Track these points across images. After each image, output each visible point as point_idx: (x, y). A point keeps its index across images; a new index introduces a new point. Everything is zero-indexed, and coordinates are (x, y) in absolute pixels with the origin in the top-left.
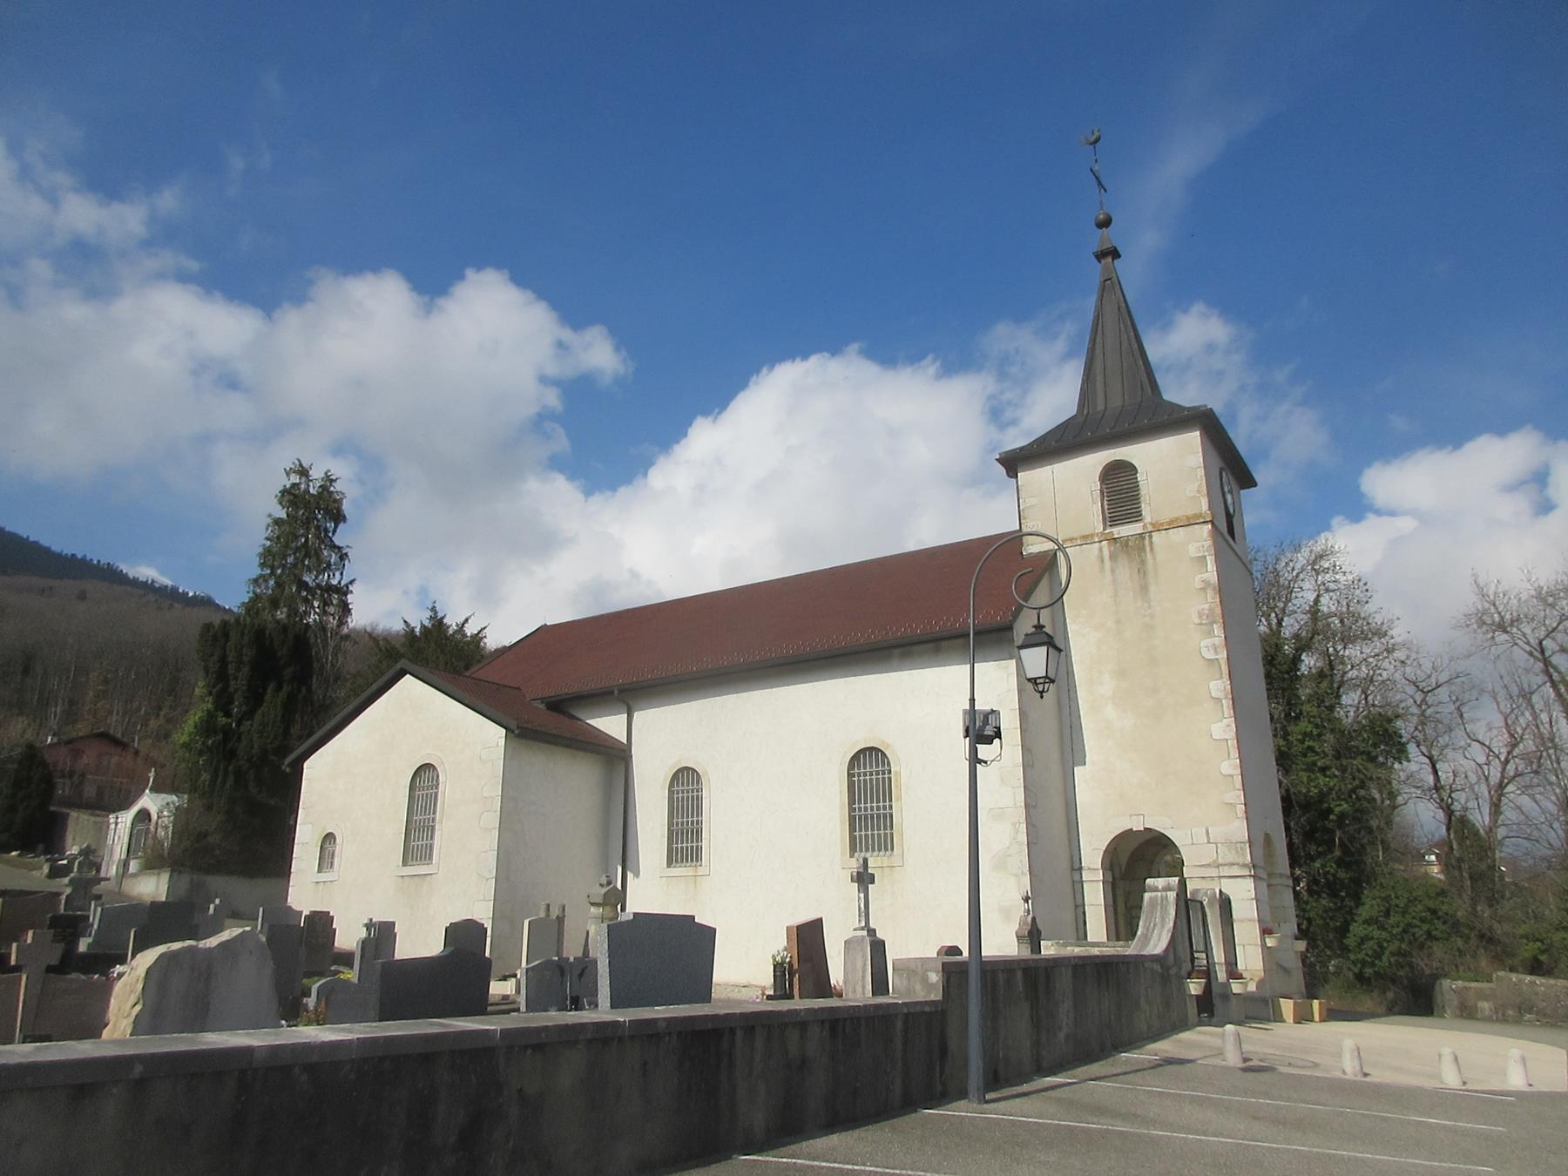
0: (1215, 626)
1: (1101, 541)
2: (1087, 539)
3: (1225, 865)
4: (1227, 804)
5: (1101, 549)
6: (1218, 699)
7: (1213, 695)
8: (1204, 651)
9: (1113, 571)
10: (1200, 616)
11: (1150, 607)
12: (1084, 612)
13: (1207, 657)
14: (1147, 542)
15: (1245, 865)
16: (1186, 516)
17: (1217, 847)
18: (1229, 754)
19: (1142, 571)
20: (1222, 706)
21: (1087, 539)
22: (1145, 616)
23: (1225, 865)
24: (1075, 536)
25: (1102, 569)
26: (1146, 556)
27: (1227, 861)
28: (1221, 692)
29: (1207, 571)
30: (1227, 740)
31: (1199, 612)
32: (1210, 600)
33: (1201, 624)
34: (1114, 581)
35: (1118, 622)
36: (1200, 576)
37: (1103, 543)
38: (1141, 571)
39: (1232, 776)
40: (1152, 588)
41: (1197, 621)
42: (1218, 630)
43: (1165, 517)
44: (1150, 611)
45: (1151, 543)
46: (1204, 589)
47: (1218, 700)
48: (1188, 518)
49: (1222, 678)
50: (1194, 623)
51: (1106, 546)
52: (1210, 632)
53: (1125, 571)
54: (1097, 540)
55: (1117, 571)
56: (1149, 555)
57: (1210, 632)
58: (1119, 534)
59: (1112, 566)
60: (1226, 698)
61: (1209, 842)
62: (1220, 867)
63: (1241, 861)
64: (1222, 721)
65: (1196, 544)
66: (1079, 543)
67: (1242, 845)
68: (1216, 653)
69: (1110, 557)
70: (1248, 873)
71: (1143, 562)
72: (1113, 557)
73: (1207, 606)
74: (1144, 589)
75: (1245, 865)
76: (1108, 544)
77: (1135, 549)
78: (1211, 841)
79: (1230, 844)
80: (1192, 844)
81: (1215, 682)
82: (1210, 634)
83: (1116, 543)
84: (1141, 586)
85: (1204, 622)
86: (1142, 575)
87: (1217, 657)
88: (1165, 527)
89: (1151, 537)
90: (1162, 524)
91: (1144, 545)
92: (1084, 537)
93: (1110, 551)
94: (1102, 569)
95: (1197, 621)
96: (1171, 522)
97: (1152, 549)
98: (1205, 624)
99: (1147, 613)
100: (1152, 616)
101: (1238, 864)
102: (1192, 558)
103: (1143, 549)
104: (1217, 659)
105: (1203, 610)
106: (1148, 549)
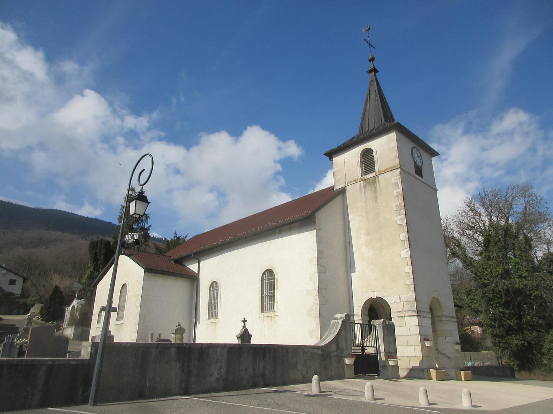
2: (355, 181)
3: (407, 311)
4: (407, 285)
5: (360, 185)
6: (403, 240)
7: (401, 239)
9: (365, 193)
10: (396, 207)
11: (378, 205)
13: (399, 224)
14: (377, 179)
15: (414, 311)
17: (403, 303)
19: (375, 192)
21: (355, 181)
22: (376, 209)
23: (407, 311)
25: (361, 193)
26: (376, 185)
27: (407, 309)
28: (404, 238)
29: (399, 188)
30: (407, 258)
31: (396, 206)
32: (399, 200)
33: (396, 210)
35: (367, 213)
36: (396, 191)
38: (375, 191)
39: (409, 273)
40: (379, 198)
41: (395, 209)
42: (403, 212)
44: (378, 207)
45: (378, 180)
46: (397, 196)
47: (403, 241)
48: (391, 168)
49: (404, 232)
53: (369, 192)
54: (359, 181)
56: (378, 185)
57: (400, 213)
59: (364, 191)
60: (406, 240)
61: (400, 302)
62: (405, 312)
63: (412, 309)
64: (405, 250)
65: (394, 178)
67: (413, 302)
68: (402, 221)
70: (415, 314)
71: (375, 188)
72: (365, 187)
73: (398, 203)
74: (376, 198)
75: (414, 311)
76: (363, 182)
77: (372, 183)
78: (401, 301)
79: (408, 302)
80: (394, 303)
81: (402, 234)
82: (400, 214)
83: (366, 181)
84: (375, 197)
85: (397, 209)
86: (375, 193)
87: (403, 223)
88: (383, 173)
89: (378, 177)
90: (382, 171)
91: (376, 181)
92: (355, 180)
93: (364, 185)
94: (361, 193)
95: (395, 209)
97: (378, 182)
98: (399, 210)
99: (377, 208)
101: (411, 310)
102: (393, 184)
104: (403, 224)
105: (397, 204)
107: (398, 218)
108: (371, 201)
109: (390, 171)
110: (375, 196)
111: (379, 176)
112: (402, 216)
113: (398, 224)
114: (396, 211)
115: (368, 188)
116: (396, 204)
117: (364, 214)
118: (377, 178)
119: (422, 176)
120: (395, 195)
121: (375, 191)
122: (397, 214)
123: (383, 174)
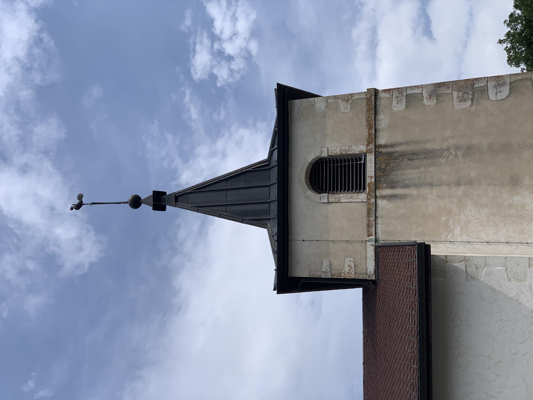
0: (475, 86)
1: (376, 195)
5: (383, 197)
8: (501, 96)
9: (406, 186)
11: (448, 149)
12: (443, 219)
13: (508, 94)
14: (384, 150)
16: (367, 111)
19: (412, 156)
22: (456, 156)
24: (365, 221)
25: (402, 197)
26: (396, 152)
29: (422, 93)
31: (460, 101)
32: (450, 91)
33: (472, 100)
34: (417, 186)
35: (458, 184)
37: (377, 194)
40: (429, 146)
41: (469, 103)
43: (363, 132)
44: (452, 151)
45: (385, 146)
46: (438, 97)
48: (369, 110)
50: (471, 105)
51: (380, 191)
54: (373, 200)
55: (407, 182)
56: (398, 149)
58: (371, 177)
65: (394, 103)
66: (372, 219)
69: (392, 187)
71: (403, 155)
72: (392, 185)
73: (455, 94)
83: (380, 181)
84: (426, 158)
85: (470, 96)
86: (415, 157)
87: (508, 82)
88: (373, 132)
89: (380, 146)
90: (370, 135)
91: (386, 153)
92: (369, 213)
93: (387, 188)
95: (469, 103)
96: (370, 128)
97: (392, 146)
98: (473, 95)
99: (454, 153)
100: (457, 148)
102: (406, 108)
103: (392, 153)
104: (510, 83)
106: (390, 150)
107: (492, 97)
108: (432, 168)
110: (422, 156)
111: (377, 144)
112: (489, 86)
113: (507, 97)
114: (475, 103)
115: (398, 175)
116: (455, 100)
117: (460, 191)
118: (380, 150)
123: (377, 134)
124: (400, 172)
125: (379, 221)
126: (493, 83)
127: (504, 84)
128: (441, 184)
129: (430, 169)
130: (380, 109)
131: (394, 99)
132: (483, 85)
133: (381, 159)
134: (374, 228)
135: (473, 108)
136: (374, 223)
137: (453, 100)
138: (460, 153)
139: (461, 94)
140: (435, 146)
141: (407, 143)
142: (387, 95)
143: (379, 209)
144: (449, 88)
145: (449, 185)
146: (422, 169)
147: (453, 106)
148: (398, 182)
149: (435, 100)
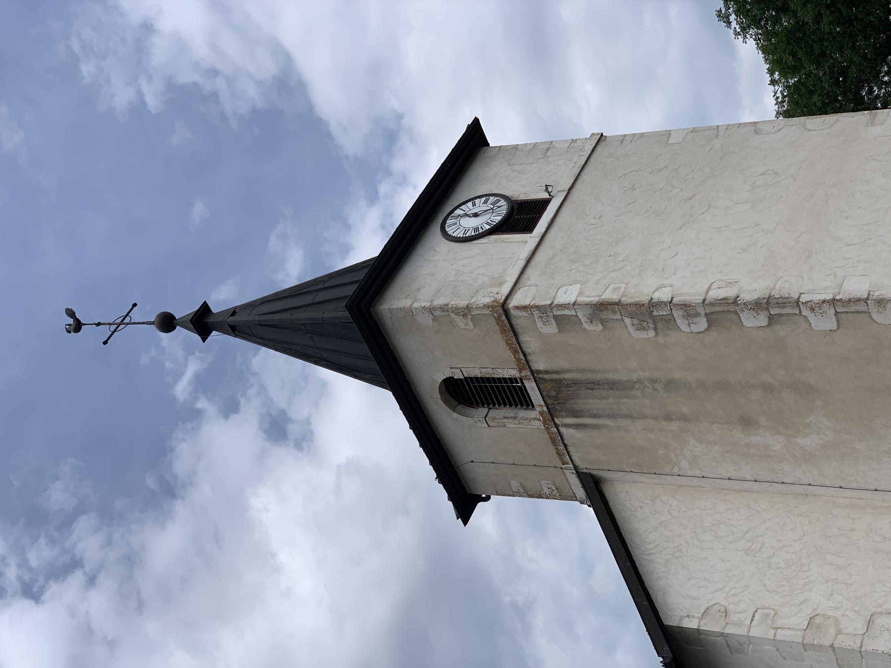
0: (655, 313)
7: (765, 324)
11: (639, 381)
18: (858, 312)
19: (593, 385)
20: (781, 315)
22: (654, 389)
32: (618, 316)
33: (655, 329)
35: (668, 418)
38: (590, 386)
40: (611, 376)
41: (652, 333)
45: (547, 372)
46: (603, 322)
48: (503, 331)
52: (665, 320)
57: (665, 320)
64: (805, 316)
65: (540, 324)
66: (562, 447)
71: (576, 383)
72: (575, 414)
74: (612, 385)
81: (743, 319)
84: (612, 389)
87: (703, 312)
89: (539, 372)
90: (518, 360)
91: (552, 380)
92: (553, 441)
97: (557, 372)
98: (655, 323)
106: (555, 376)
109: (516, 335)
113: (706, 330)
115: (579, 404)
116: (631, 329)
118: (541, 376)
119: (542, 205)
120: (599, 328)
121: (590, 386)
122: (669, 329)
123: (529, 358)
124: (580, 401)
125: (570, 449)
126: (681, 312)
127: (697, 315)
128: (644, 417)
129: (622, 400)
130: (519, 329)
131: (537, 320)
132: (665, 313)
133: (545, 386)
134: (568, 457)
135: (660, 339)
136: (565, 452)
137: (626, 327)
138: (659, 387)
139: (636, 321)
140: (622, 376)
141: (578, 371)
142: (524, 314)
143: (565, 437)
144: (615, 313)
145: (655, 418)
146: (611, 400)
147: (630, 335)
148: (581, 411)
149: (600, 325)
